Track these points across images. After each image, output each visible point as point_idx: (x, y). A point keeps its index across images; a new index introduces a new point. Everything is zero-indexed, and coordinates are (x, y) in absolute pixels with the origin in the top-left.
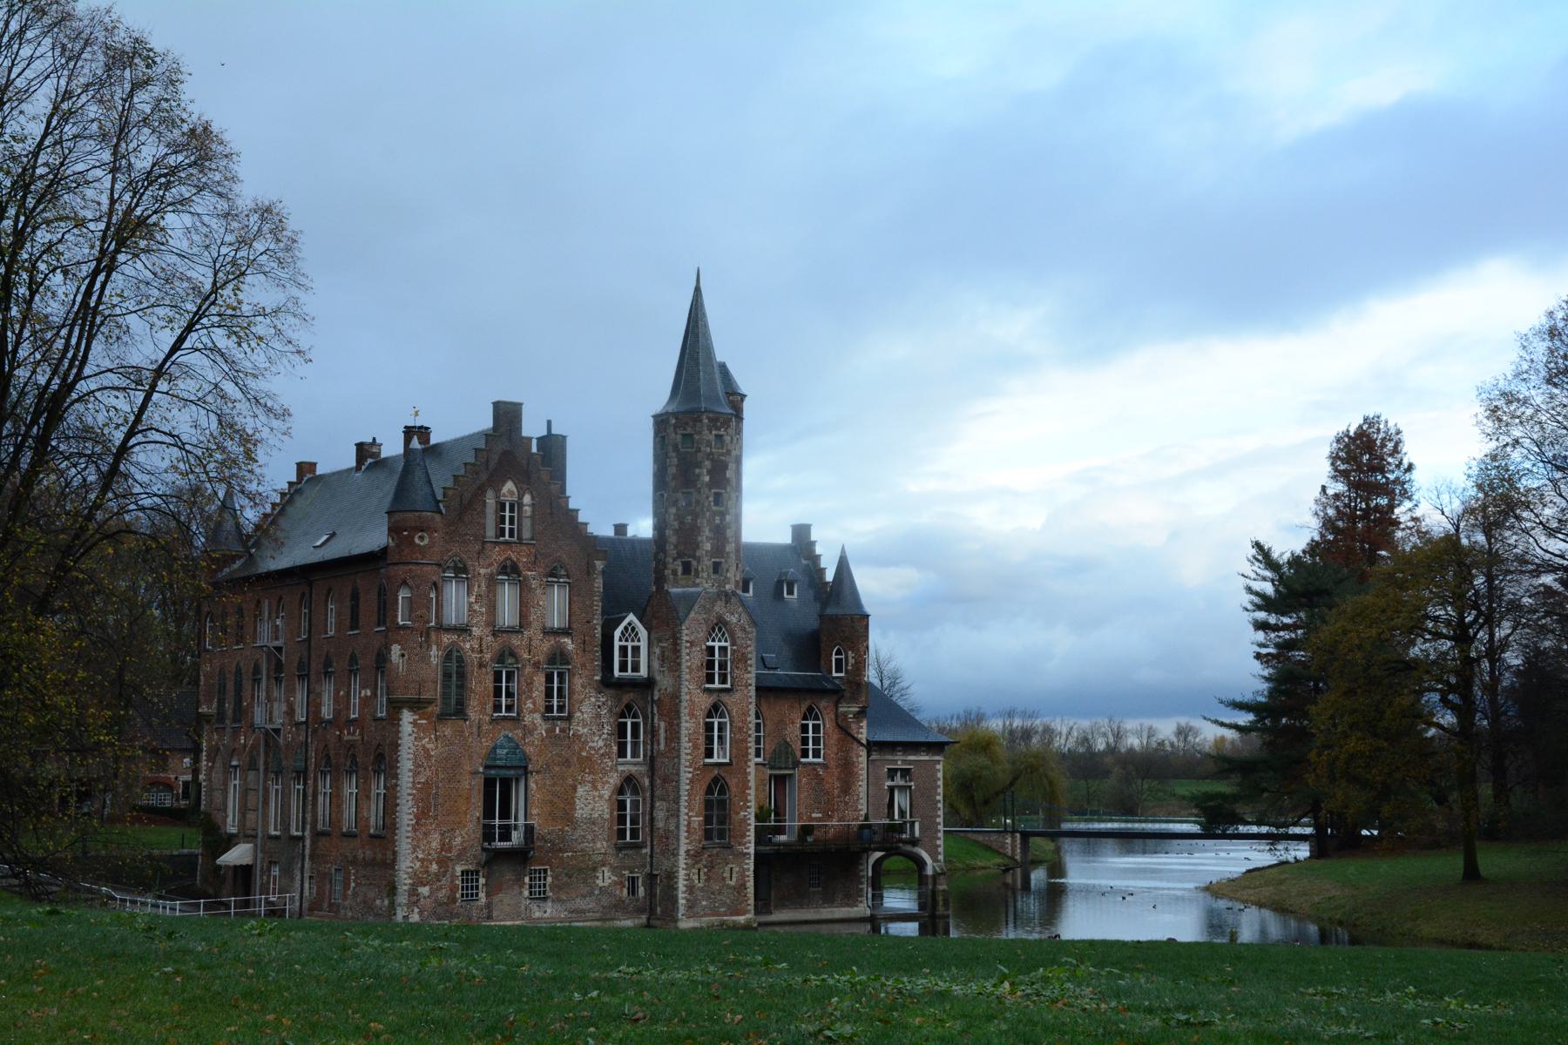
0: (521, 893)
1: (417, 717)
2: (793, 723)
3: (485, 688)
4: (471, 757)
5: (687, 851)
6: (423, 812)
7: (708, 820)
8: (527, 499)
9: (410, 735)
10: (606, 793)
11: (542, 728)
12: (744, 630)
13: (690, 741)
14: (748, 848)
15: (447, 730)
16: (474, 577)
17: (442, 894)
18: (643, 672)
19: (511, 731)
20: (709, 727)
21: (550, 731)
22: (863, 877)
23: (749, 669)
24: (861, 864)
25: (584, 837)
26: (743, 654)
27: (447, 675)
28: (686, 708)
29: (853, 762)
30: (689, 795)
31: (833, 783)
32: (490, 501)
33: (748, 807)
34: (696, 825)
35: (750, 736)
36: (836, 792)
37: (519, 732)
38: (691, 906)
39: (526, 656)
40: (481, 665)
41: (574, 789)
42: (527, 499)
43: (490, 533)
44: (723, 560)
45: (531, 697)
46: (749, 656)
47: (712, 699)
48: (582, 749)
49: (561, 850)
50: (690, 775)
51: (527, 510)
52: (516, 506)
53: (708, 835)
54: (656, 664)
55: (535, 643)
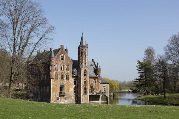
7: (84, 91)
8: (64, 56)
10: (73, 88)
11: (66, 81)
15: (56, 81)
17: (55, 99)
18: (77, 75)
20: (84, 81)
27: (56, 75)
31: (97, 88)
32: (60, 56)
38: (82, 101)
42: (64, 56)
43: (60, 60)
47: (84, 78)
51: (64, 57)
52: (63, 57)
53: (84, 93)
54: (78, 74)
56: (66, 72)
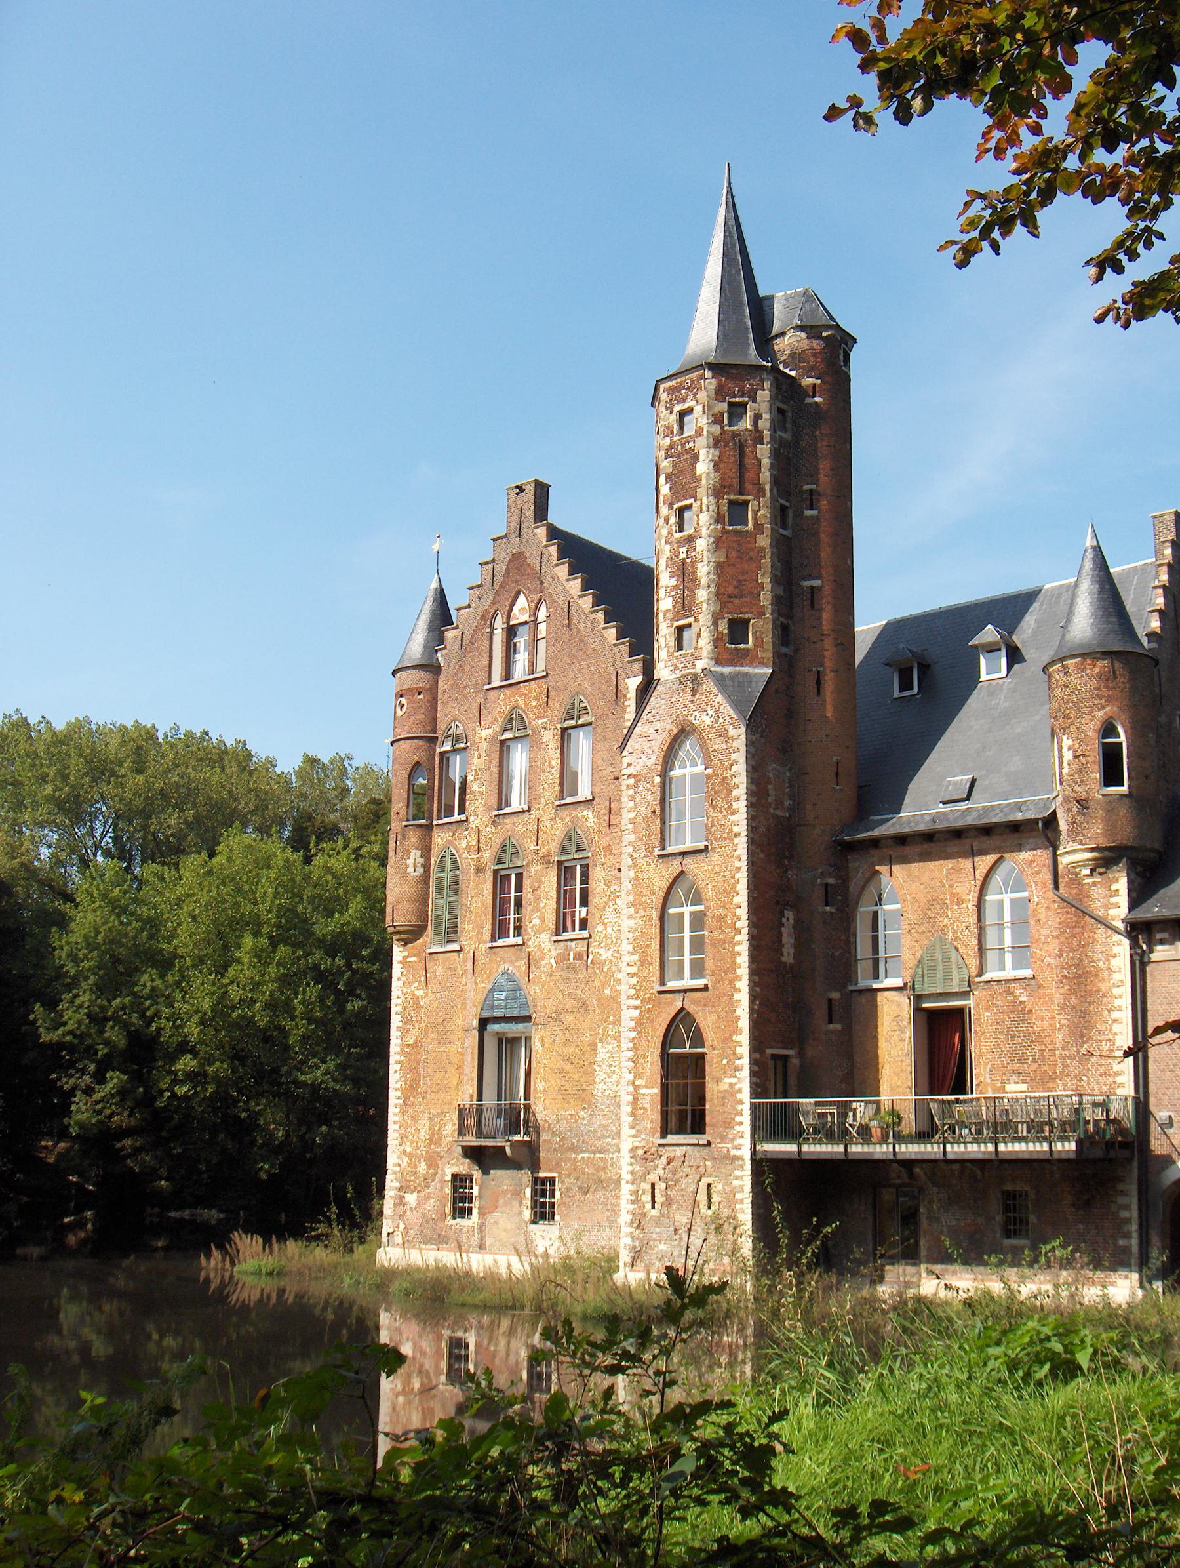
0: (521, 1213)
1: (406, 954)
2: (959, 902)
3: (483, 902)
4: (464, 1005)
5: (634, 1149)
6: (411, 1086)
9: (399, 979)
12: (724, 734)
13: (635, 951)
14: (738, 1147)
16: (474, 743)
19: (512, 963)
21: (562, 958)
22: (1128, 1221)
23: (735, 805)
24: (1123, 1193)
25: (605, 1127)
26: (724, 779)
28: (629, 893)
29: (1097, 969)
30: (635, 1048)
33: (736, 1069)
34: (645, 1103)
35: (739, 931)
36: (1059, 1037)
37: (522, 965)
39: (533, 847)
40: (479, 870)
41: (594, 1049)
44: (691, 620)
45: (538, 910)
46: (735, 781)
47: (675, 866)
48: (603, 986)
49: (573, 1149)
50: (636, 1013)
55: (546, 823)
56: (555, 832)
